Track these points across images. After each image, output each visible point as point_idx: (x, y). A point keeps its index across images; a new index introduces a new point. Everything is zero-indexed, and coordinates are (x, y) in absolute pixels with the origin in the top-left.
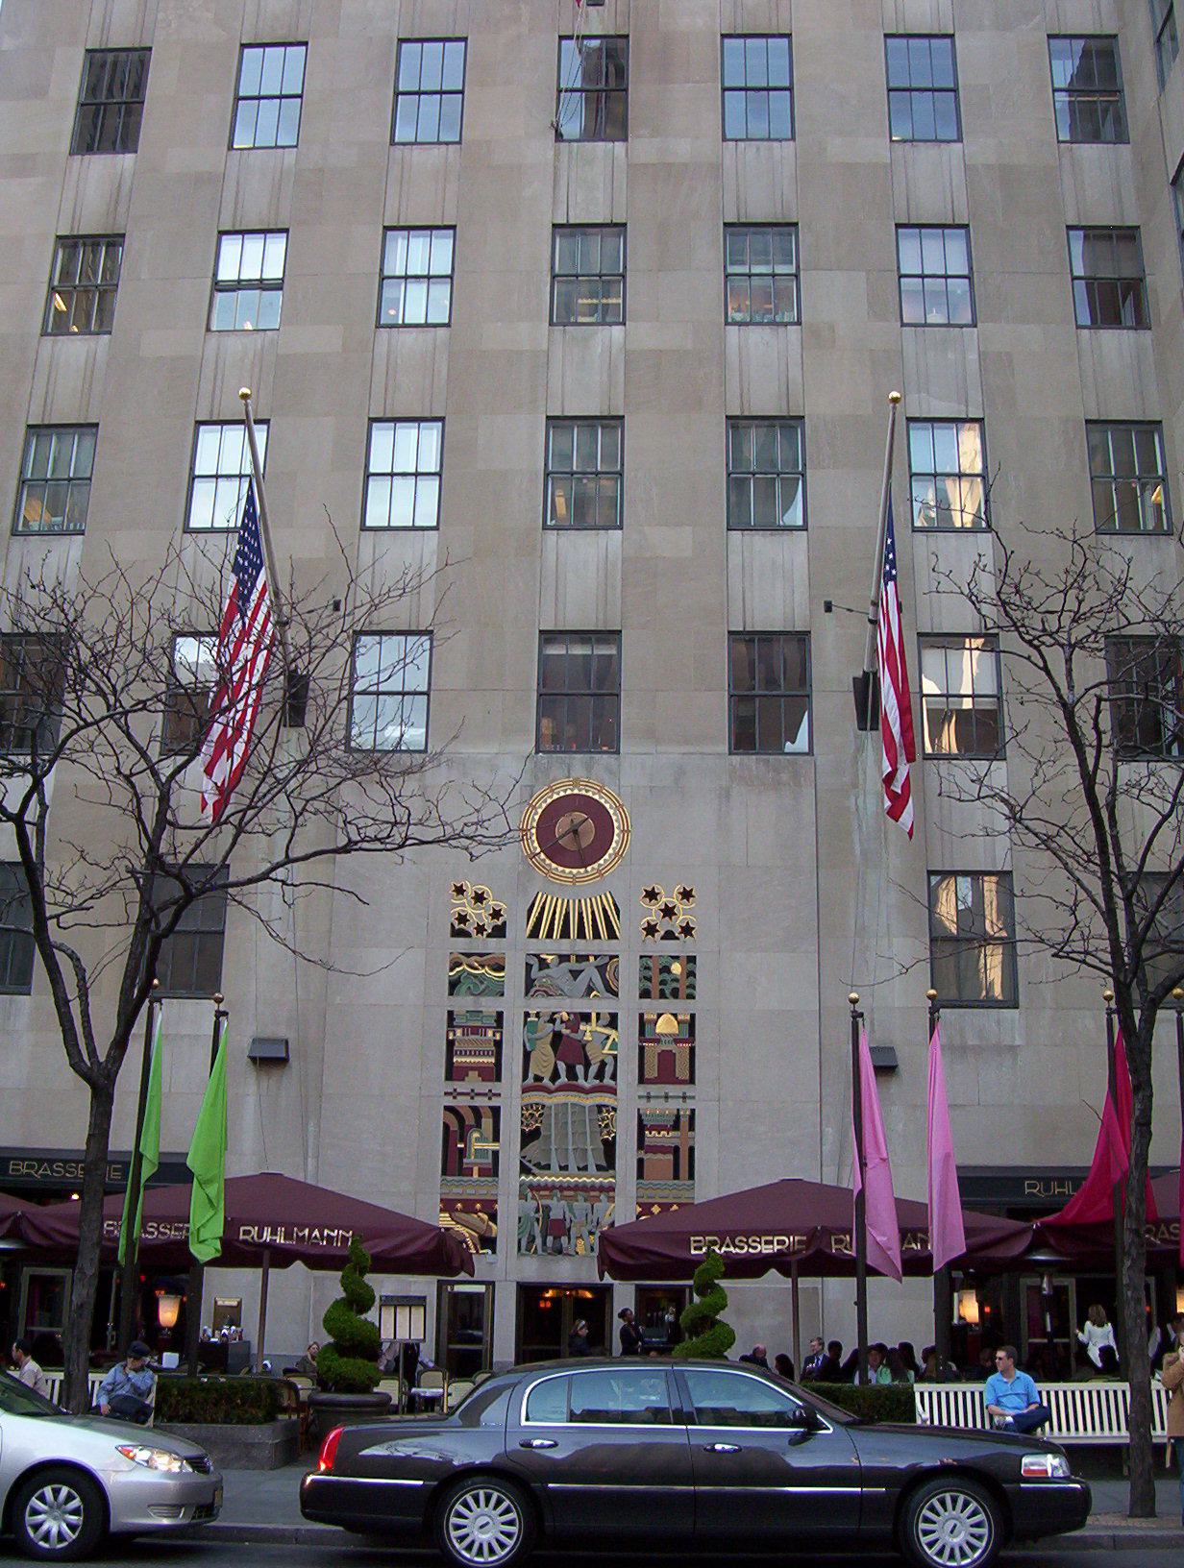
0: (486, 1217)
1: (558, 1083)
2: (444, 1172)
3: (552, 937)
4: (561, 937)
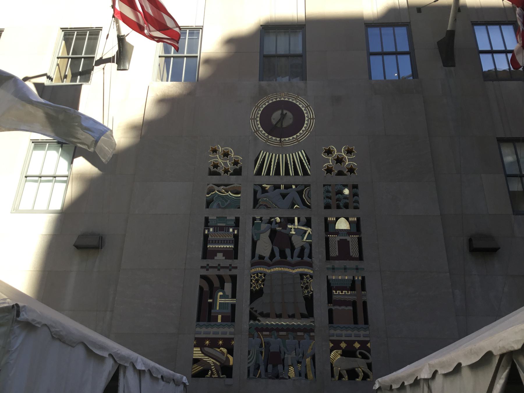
0: (225, 350)
1: (274, 260)
2: (198, 320)
3: (269, 175)
4: (275, 175)
